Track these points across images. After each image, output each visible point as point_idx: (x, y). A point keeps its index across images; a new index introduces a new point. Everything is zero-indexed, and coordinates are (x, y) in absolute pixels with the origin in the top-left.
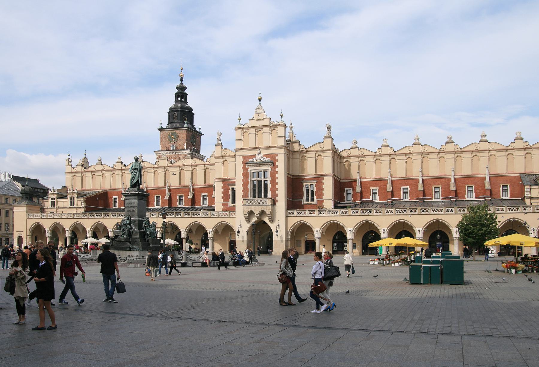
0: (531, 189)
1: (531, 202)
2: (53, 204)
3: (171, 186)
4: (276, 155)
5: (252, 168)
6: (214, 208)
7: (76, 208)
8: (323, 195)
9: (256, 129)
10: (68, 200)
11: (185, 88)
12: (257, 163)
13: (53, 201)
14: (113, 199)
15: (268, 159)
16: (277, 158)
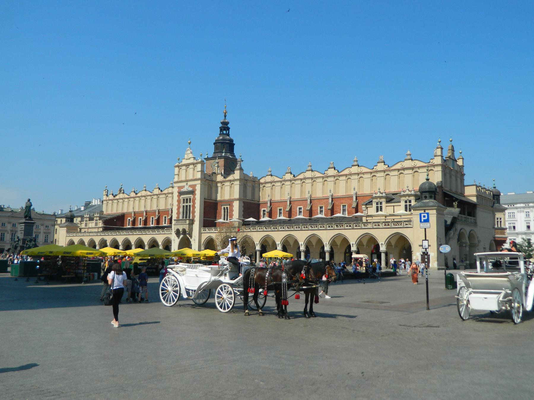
1: (367, 219)
2: (86, 225)
10: (94, 222)
14: (128, 220)
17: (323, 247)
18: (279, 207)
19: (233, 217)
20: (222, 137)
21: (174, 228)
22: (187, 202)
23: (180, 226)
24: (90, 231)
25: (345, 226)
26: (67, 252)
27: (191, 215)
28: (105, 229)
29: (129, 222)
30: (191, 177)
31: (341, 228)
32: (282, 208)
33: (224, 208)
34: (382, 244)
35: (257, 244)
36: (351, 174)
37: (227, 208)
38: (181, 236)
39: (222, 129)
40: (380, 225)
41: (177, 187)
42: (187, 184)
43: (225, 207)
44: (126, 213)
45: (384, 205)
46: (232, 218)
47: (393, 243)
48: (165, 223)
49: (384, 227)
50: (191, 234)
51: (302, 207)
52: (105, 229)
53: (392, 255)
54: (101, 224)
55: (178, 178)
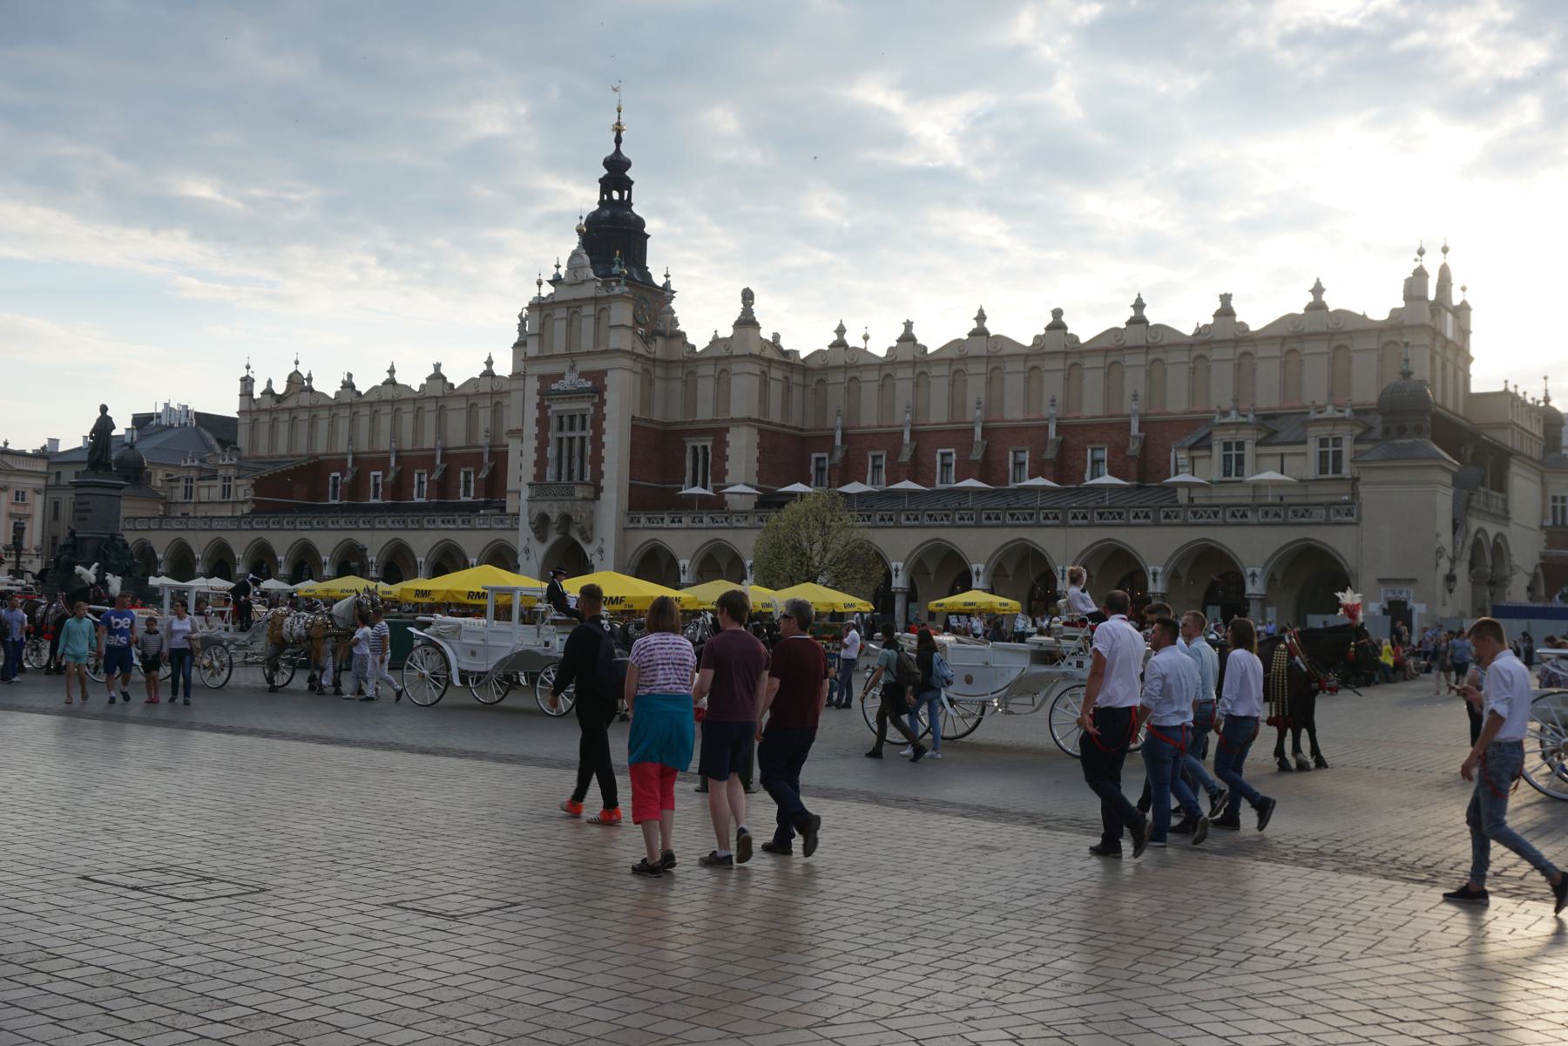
0: (1193, 459)
2: (188, 492)
3: (450, 445)
4: (604, 373)
5: (556, 407)
6: (502, 505)
7: (233, 502)
8: (726, 473)
9: (568, 308)
10: (219, 483)
11: (628, 164)
12: (564, 392)
13: (227, 483)
14: (331, 479)
15: (589, 384)
16: (607, 381)
17: (888, 576)
18: (875, 449)
19: (727, 478)
20: (608, 212)
21: (530, 512)
22: (572, 428)
23: (550, 506)
24: (204, 514)
25: (1128, 516)
26: (611, 598)
27: (588, 468)
28: (263, 510)
29: (335, 486)
30: (587, 344)
31: (1115, 521)
32: (884, 454)
33: (695, 448)
34: (1254, 575)
35: (978, 573)
36: (1121, 350)
37: (705, 448)
38: (554, 537)
39: (606, 185)
40: (1249, 514)
41: (536, 378)
42: (572, 368)
43: (699, 444)
44: (327, 455)
45: (1249, 451)
46: (723, 481)
47: (1278, 576)
48: (467, 494)
49: (1262, 520)
50: (588, 534)
51: (953, 450)
52: (263, 510)
53: (1274, 609)
54: (243, 490)
55: (541, 345)
